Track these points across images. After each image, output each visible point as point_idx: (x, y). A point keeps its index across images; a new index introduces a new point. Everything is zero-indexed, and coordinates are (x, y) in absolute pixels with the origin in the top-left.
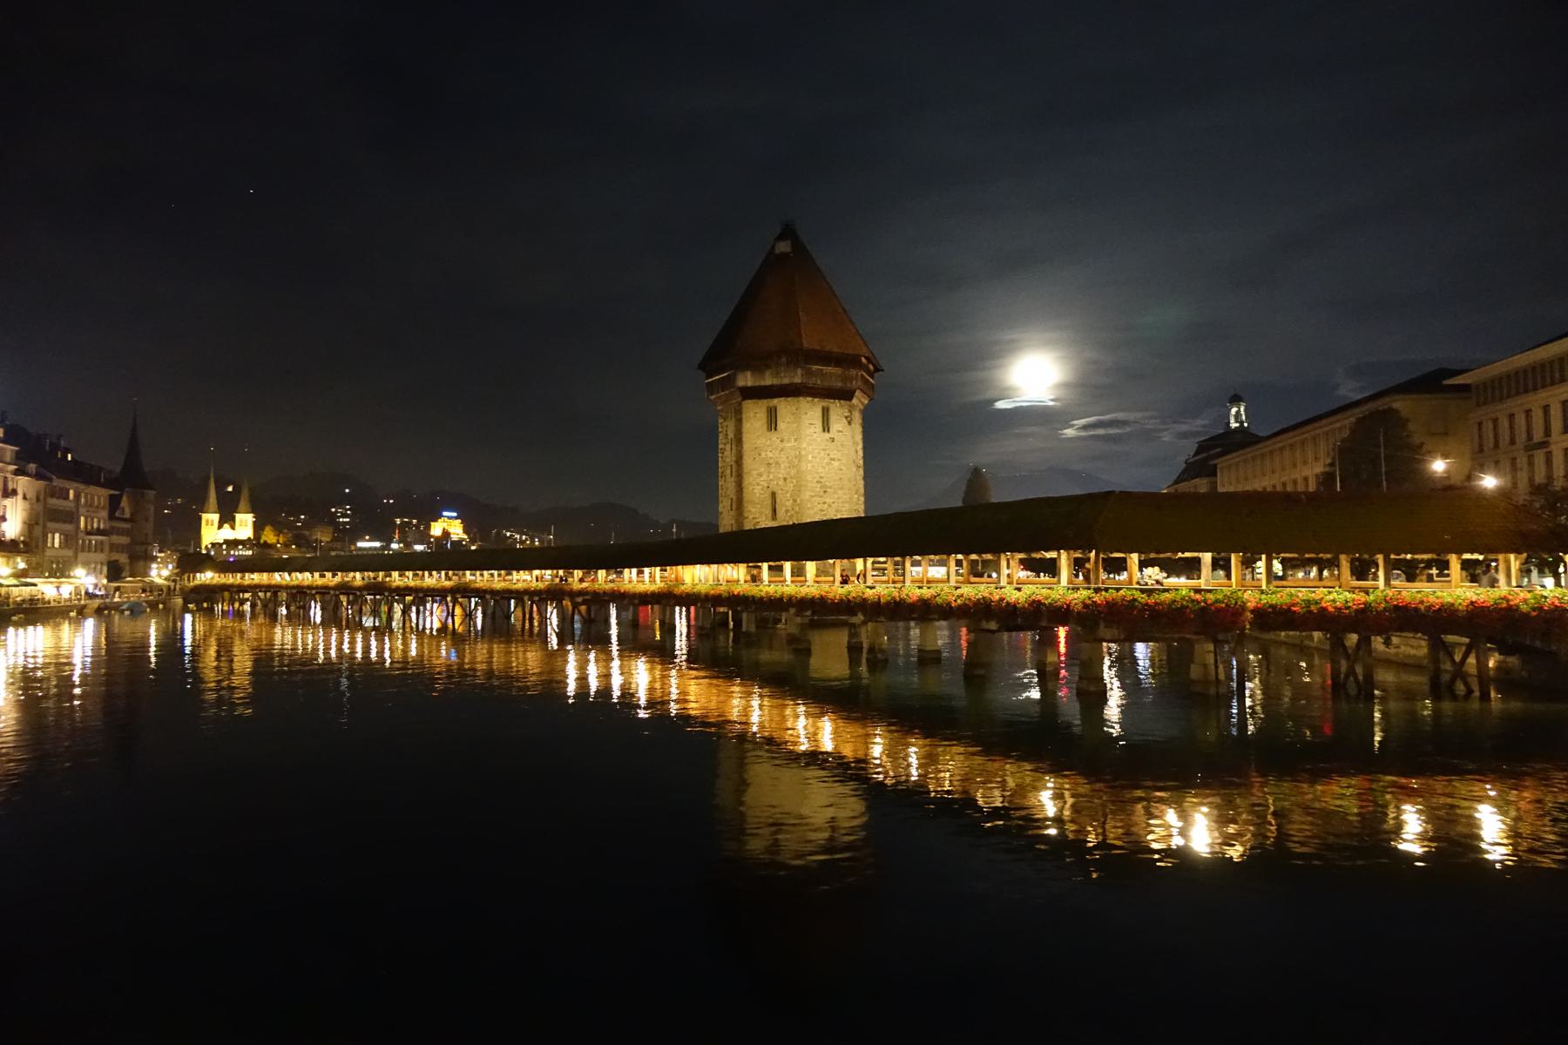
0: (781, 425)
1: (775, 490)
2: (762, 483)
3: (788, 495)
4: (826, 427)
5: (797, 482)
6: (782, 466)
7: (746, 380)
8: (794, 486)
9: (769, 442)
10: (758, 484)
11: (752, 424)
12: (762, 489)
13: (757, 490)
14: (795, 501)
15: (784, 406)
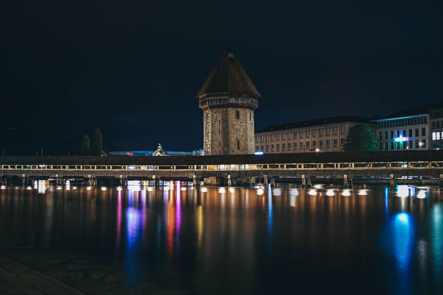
0: (241, 118)
1: (239, 139)
2: (235, 137)
3: (243, 141)
4: (250, 120)
5: (246, 137)
6: (241, 132)
7: (232, 101)
8: (245, 139)
9: (237, 123)
10: (233, 137)
11: (231, 116)
12: (235, 139)
13: (233, 139)
14: (245, 143)
15: (241, 111)
